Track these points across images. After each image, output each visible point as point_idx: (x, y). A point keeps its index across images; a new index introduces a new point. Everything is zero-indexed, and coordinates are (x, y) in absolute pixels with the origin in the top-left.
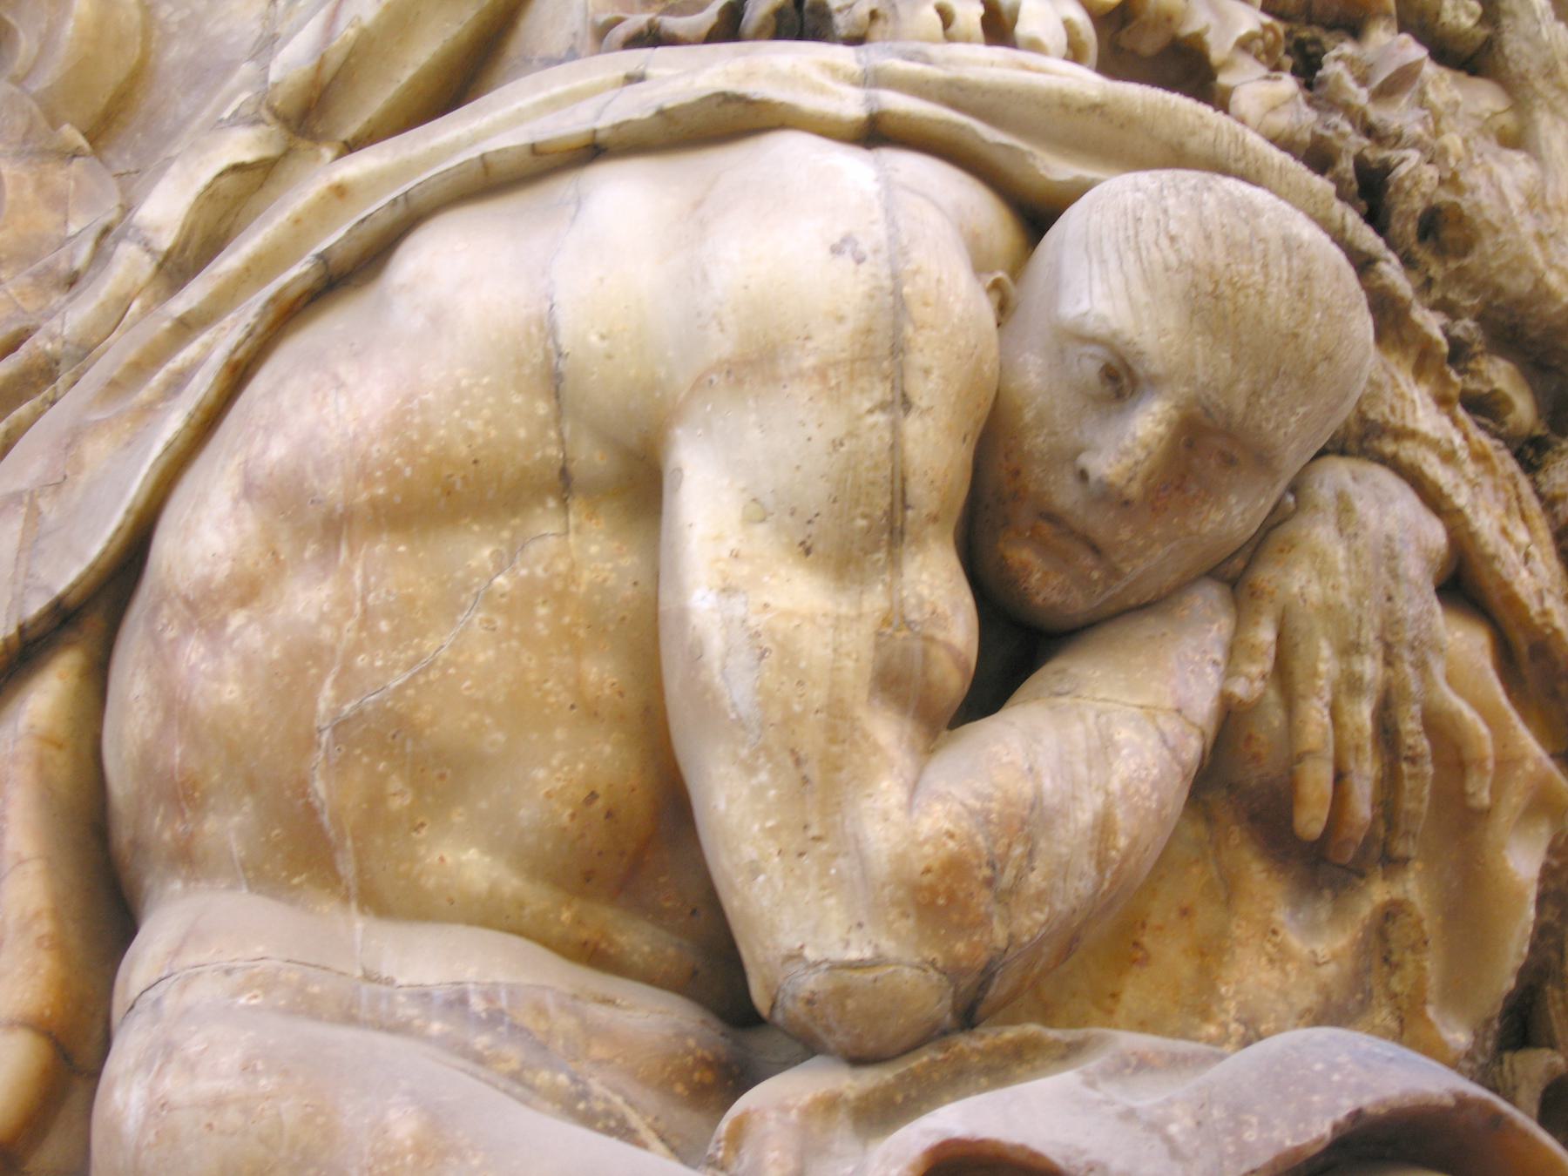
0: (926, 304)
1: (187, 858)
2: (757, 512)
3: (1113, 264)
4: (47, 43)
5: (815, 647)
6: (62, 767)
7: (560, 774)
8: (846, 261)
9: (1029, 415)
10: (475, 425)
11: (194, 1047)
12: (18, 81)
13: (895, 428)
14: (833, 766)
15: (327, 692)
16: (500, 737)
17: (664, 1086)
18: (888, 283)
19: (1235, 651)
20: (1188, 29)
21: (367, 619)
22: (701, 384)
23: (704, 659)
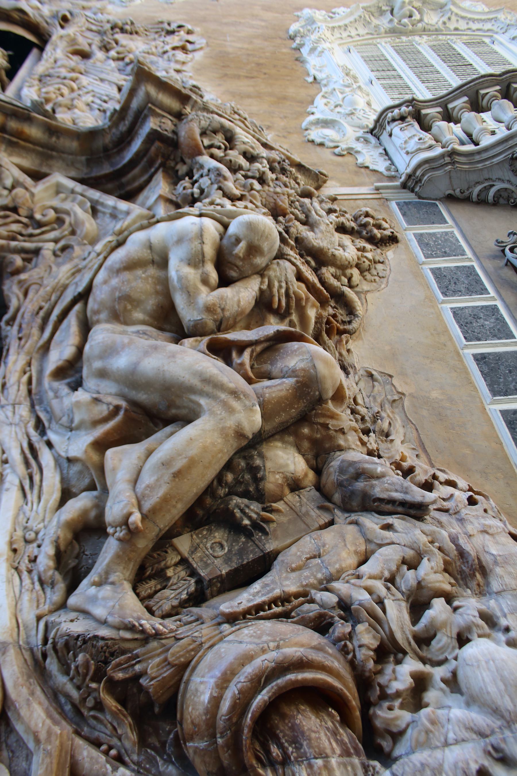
2: (181, 260)
6: (81, 316)
19: (262, 283)
21: (123, 282)
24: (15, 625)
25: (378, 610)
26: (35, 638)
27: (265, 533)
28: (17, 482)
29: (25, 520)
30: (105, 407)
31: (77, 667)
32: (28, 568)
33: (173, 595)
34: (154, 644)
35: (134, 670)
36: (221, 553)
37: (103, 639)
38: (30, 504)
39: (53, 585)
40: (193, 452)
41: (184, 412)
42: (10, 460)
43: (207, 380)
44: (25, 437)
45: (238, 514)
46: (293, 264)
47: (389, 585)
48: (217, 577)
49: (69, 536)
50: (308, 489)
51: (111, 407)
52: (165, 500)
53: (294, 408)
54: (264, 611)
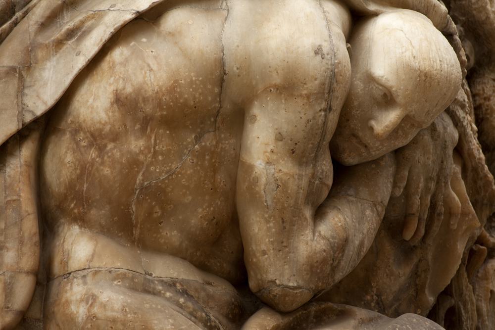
0: (341, 75)
2: (279, 137)
5: (292, 186)
8: (319, 58)
13: (326, 116)
14: (292, 224)
16: (190, 198)
22: (267, 90)
23: (258, 184)
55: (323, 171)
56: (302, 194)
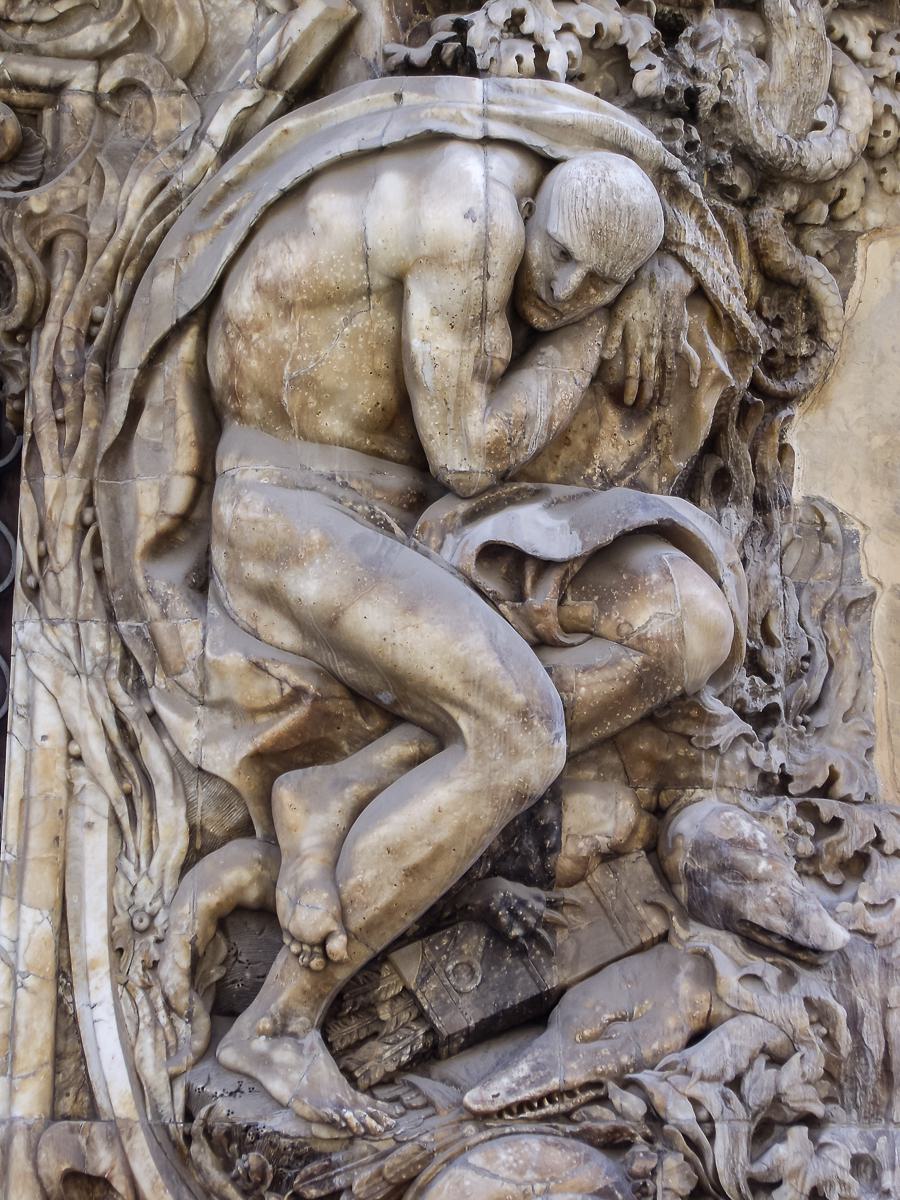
1: (239, 415)
3: (566, 216)
4: (169, 39)
5: (453, 363)
7: (368, 395)
9: (535, 264)
10: (338, 275)
11: (247, 499)
12: (157, 56)
14: (458, 404)
15: (287, 368)
17: (400, 506)
18: (484, 231)
19: (606, 338)
20: (621, 42)
24: (137, 1087)
25: (700, 1134)
26: (169, 1109)
27: (548, 951)
28: (106, 811)
29: (130, 889)
30: (274, 684)
31: (247, 1170)
32: (143, 982)
33: (388, 1054)
34: (362, 1146)
35: (332, 1184)
36: (471, 987)
37: (286, 1136)
38: (133, 855)
39: (190, 1018)
40: (443, 835)
41: (426, 719)
42: (85, 756)
43: (475, 684)
44: (110, 707)
45: (504, 920)
46: (688, 268)
47: (731, 1094)
48: (461, 1032)
49: (211, 930)
50: (633, 857)
51: (287, 690)
52: (389, 911)
53: (631, 712)
54: (532, 1108)
55: (491, 344)
56: (467, 372)
